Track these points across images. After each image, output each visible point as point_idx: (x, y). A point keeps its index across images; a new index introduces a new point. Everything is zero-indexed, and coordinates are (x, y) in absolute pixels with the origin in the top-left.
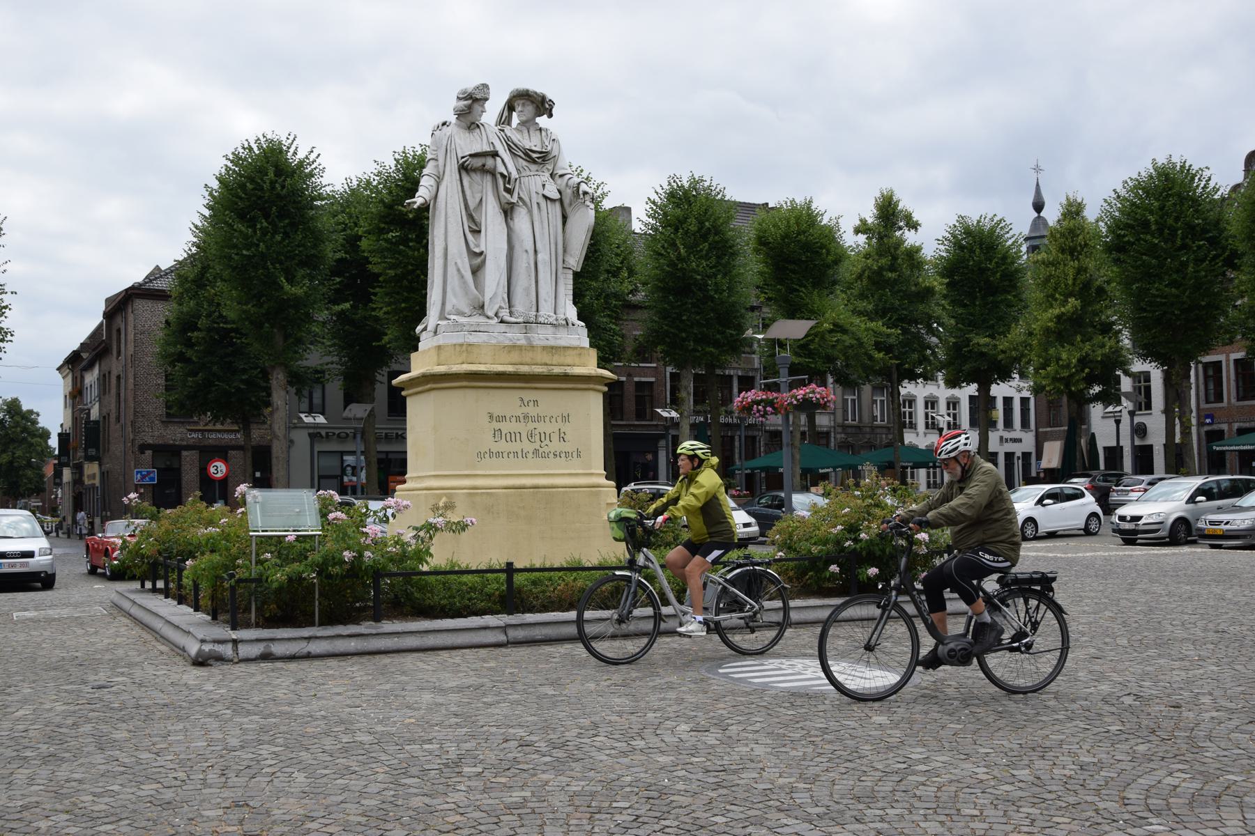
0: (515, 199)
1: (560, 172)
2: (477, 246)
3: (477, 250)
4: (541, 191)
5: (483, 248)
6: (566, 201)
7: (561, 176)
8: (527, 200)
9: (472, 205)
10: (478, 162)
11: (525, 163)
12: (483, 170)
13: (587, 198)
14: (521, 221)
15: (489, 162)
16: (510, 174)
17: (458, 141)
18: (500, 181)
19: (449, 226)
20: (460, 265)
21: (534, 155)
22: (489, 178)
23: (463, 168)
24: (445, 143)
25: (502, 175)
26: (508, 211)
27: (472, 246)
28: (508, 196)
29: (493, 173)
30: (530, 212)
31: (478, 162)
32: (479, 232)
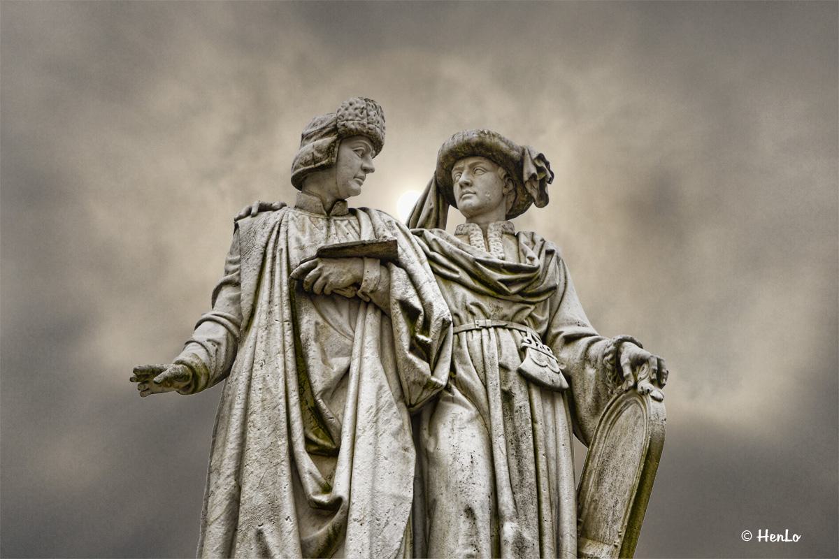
0: (442, 377)
1: (568, 330)
2: (327, 489)
3: (324, 498)
4: (513, 362)
5: (340, 489)
6: (586, 401)
7: (570, 339)
8: (477, 385)
9: (319, 381)
10: (338, 274)
11: (471, 298)
12: (357, 299)
13: (643, 373)
14: (458, 436)
15: (372, 273)
16: (428, 307)
17: (293, 231)
18: (402, 326)
19: (252, 434)
20: (271, 540)
21: (497, 276)
22: (368, 325)
23: (303, 291)
24: (260, 241)
25: (405, 305)
26: (422, 410)
27: (310, 486)
28: (423, 366)
29: (379, 304)
30: (484, 415)
31: (338, 274)
32: (333, 454)
